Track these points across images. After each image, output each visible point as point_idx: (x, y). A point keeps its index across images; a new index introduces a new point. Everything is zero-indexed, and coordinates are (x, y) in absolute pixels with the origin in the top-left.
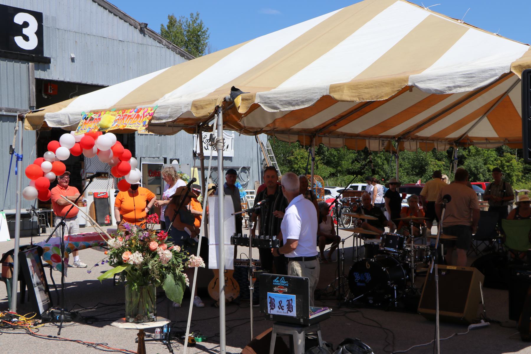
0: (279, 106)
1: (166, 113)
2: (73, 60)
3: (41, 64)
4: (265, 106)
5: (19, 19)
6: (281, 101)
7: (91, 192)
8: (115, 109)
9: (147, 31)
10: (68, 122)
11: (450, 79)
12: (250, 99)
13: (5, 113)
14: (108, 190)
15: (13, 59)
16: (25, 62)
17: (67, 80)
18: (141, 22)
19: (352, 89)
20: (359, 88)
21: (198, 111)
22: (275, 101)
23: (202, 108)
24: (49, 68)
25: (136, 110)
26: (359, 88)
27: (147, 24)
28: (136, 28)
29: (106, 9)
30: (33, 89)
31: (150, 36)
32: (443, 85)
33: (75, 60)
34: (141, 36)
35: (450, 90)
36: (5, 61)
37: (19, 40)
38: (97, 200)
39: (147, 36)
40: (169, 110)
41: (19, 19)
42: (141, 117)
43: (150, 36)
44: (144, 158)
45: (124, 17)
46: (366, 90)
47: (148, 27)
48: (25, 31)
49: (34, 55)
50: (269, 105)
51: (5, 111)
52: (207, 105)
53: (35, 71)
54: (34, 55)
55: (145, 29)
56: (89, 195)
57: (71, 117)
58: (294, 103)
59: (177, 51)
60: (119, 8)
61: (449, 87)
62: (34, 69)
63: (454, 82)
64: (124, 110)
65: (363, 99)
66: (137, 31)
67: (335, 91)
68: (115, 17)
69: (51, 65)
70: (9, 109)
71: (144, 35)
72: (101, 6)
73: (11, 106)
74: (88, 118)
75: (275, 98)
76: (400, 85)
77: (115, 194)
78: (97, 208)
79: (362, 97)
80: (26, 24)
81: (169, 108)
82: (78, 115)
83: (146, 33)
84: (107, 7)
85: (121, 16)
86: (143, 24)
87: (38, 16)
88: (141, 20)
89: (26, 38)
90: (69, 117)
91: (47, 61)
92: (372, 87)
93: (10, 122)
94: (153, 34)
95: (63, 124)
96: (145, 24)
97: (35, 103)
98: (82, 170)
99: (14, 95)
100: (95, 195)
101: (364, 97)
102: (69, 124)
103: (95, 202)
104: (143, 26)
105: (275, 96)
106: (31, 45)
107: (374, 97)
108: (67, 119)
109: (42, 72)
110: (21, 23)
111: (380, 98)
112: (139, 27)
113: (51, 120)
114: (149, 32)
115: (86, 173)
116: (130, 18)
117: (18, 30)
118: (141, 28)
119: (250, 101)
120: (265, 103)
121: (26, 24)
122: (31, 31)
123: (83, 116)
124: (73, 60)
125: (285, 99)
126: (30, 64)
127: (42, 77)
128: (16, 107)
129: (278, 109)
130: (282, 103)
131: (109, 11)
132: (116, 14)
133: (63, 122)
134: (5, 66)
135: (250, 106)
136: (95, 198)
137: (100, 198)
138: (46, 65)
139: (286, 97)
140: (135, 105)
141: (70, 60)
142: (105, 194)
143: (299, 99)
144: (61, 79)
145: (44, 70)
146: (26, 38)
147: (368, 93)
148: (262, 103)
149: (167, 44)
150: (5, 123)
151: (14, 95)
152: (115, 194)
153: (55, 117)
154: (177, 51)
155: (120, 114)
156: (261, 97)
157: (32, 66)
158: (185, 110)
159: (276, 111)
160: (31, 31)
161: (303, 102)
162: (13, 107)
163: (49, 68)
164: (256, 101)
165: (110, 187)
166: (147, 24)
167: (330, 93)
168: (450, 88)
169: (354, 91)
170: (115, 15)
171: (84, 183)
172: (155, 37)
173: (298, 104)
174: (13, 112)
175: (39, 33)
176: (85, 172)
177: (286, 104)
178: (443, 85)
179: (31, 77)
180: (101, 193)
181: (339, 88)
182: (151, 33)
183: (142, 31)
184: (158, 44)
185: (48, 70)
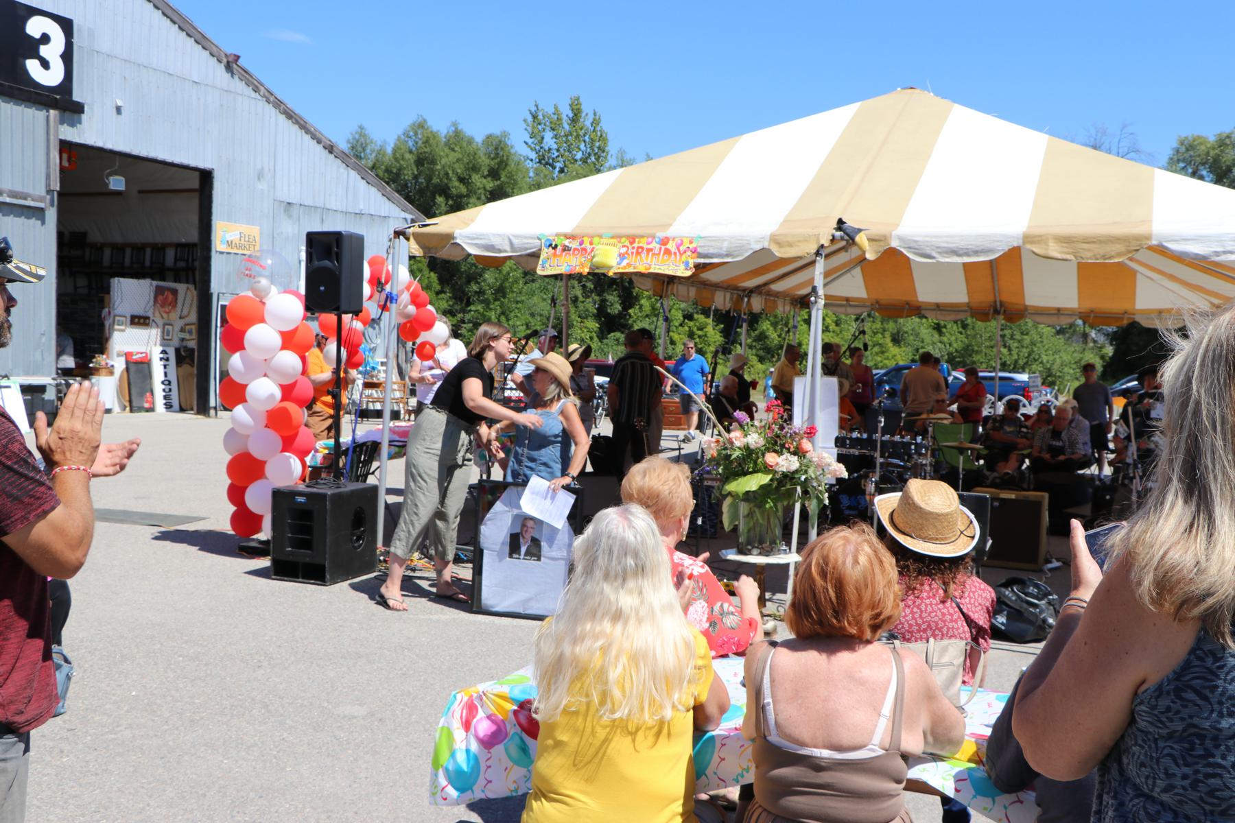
0: (934, 254)
1: (721, 248)
2: (119, 110)
3: (67, 114)
4: (908, 252)
5: (35, 27)
6: (938, 247)
7: (122, 350)
8: (610, 235)
9: (238, 68)
10: (508, 248)
11: (1217, 241)
12: (881, 240)
13: (8, 200)
14: (149, 348)
15: (23, 100)
16: (41, 107)
17: (109, 146)
18: (229, 52)
19: (1061, 242)
20: (1073, 242)
21: (783, 250)
22: (928, 246)
23: (790, 245)
24: (80, 123)
25: (657, 240)
26: (1073, 242)
27: (238, 57)
28: (220, 61)
29: (174, 22)
30: (55, 158)
31: (242, 78)
32: (1206, 249)
33: (123, 111)
34: (227, 76)
35: (1218, 256)
36: (9, 103)
37: (32, 66)
38: (133, 368)
39: (236, 77)
40: (725, 244)
41: (35, 27)
42: (675, 253)
43: (242, 78)
44: (223, 294)
45: (202, 41)
46: (1085, 246)
47: (240, 62)
48: (44, 50)
49: (58, 97)
50: (917, 251)
51: (9, 196)
52: (799, 241)
53: (60, 126)
54: (58, 97)
55: (235, 66)
56: (119, 355)
57: (515, 241)
58: (961, 252)
59: (282, 108)
60: (195, 24)
61: (1216, 252)
62: (58, 122)
63: (1223, 246)
64: (632, 240)
65: (1081, 257)
66: (222, 67)
67: (1032, 243)
68: (188, 39)
69: (84, 117)
70: (15, 192)
71: (232, 76)
72: (168, 17)
73: (18, 188)
74: (556, 246)
75: (927, 242)
76: (1139, 243)
77: (162, 356)
78: (132, 381)
79: (1079, 255)
80: (45, 39)
81: (725, 240)
82: (532, 238)
83: (235, 71)
84: (176, 19)
85: (198, 37)
86: (233, 56)
87: (66, 25)
88: (229, 48)
89: (45, 64)
90: (510, 241)
91: (78, 109)
92: (1093, 242)
93: (15, 216)
94: (245, 75)
95: (500, 251)
96: (235, 55)
97: (58, 185)
98: (107, 310)
99: (23, 167)
100: (128, 355)
101: (1082, 255)
102: (512, 252)
103: (127, 369)
104: (230, 59)
105: (927, 239)
106: (51, 77)
107: (1098, 256)
108: (507, 242)
109: (70, 129)
110: (37, 36)
111: (1110, 258)
112: (225, 60)
113: (470, 241)
114: (240, 70)
115: (115, 316)
116: (212, 43)
117: (32, 47)
118: (228, 62)
119: (882, 243)
120: (910, 248)
121: (45, 39)
122: (53, 51)
123: (543, 241)
124: (119, 110)
125: (946, 245)
126: (52, 112)
127: (69, 138)
128: (26, 190)
129: (934, 258)
130: (939, 250)
131: (180, 28)
132: (189, 32)
133: (497, 247)
134: (9, 112)
135: (882, 250)
136: (127, 362)
137: (137, 363)
138: (76, 116)
139: (948, 243)
140: (653, 231)
141: (115, 110)
142: (144, 355)
143: (970, 247)
144: (99, 144)
145: (72, 125)
146: (45, 64)
147: (1089, 250)
148: (904, 248)
149: (267, 94)
150: (6, 218)
151: (23, 167)
152: (162, 356)
153: (477, 238)
154: (282, 108)
155: (626, 244)
156: (900, 238)
157: (55, 116)
158: (758, 247)
159: (928, 260)
160: (53, 51)
161: (976, 253)
162: (21, 190)
163: (80, 123)
164: (895, 244)
165: (152, 343)
166: (238, 57)
167: (1024, 243)
168: (1217, 254)
169: (1064, 245)
170: (189, 35)
171: (109, 333)
172: (248, 80)
173: (967, 254)
174: (21, 198)
175: (67, 57)
176: (112, 315)
177: (946, 253)
178: (1206, 249)
179: (52, 137)
180: (138, 353)
181: (1040, 239)
182: (243, 73)
183: (228, 68)
184: (253, 94)
185: (78, 125)
